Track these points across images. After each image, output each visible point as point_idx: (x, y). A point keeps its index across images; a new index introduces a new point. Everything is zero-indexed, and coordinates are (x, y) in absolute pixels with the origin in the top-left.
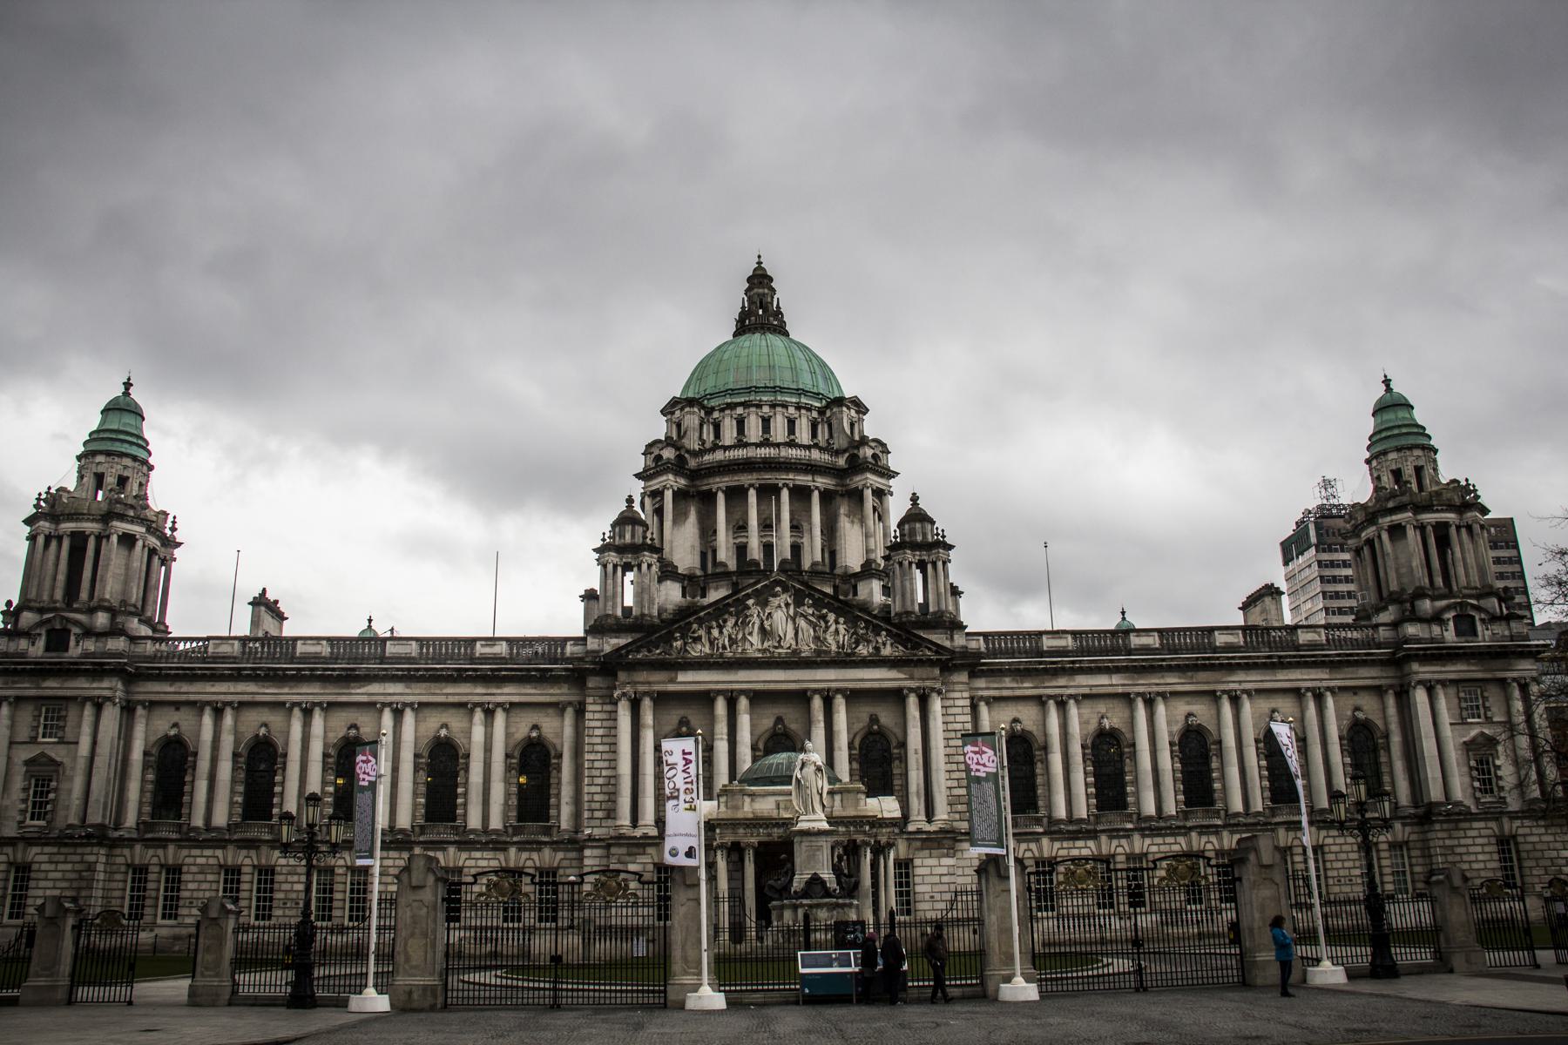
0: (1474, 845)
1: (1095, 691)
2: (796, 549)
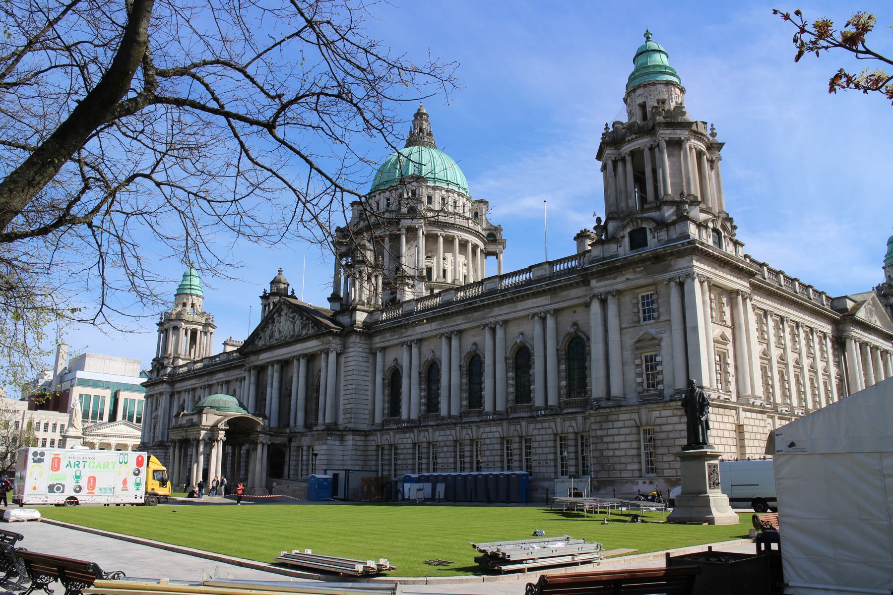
0: (619, 435)
1: (424, 335)
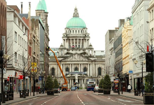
2: (79, 46)
